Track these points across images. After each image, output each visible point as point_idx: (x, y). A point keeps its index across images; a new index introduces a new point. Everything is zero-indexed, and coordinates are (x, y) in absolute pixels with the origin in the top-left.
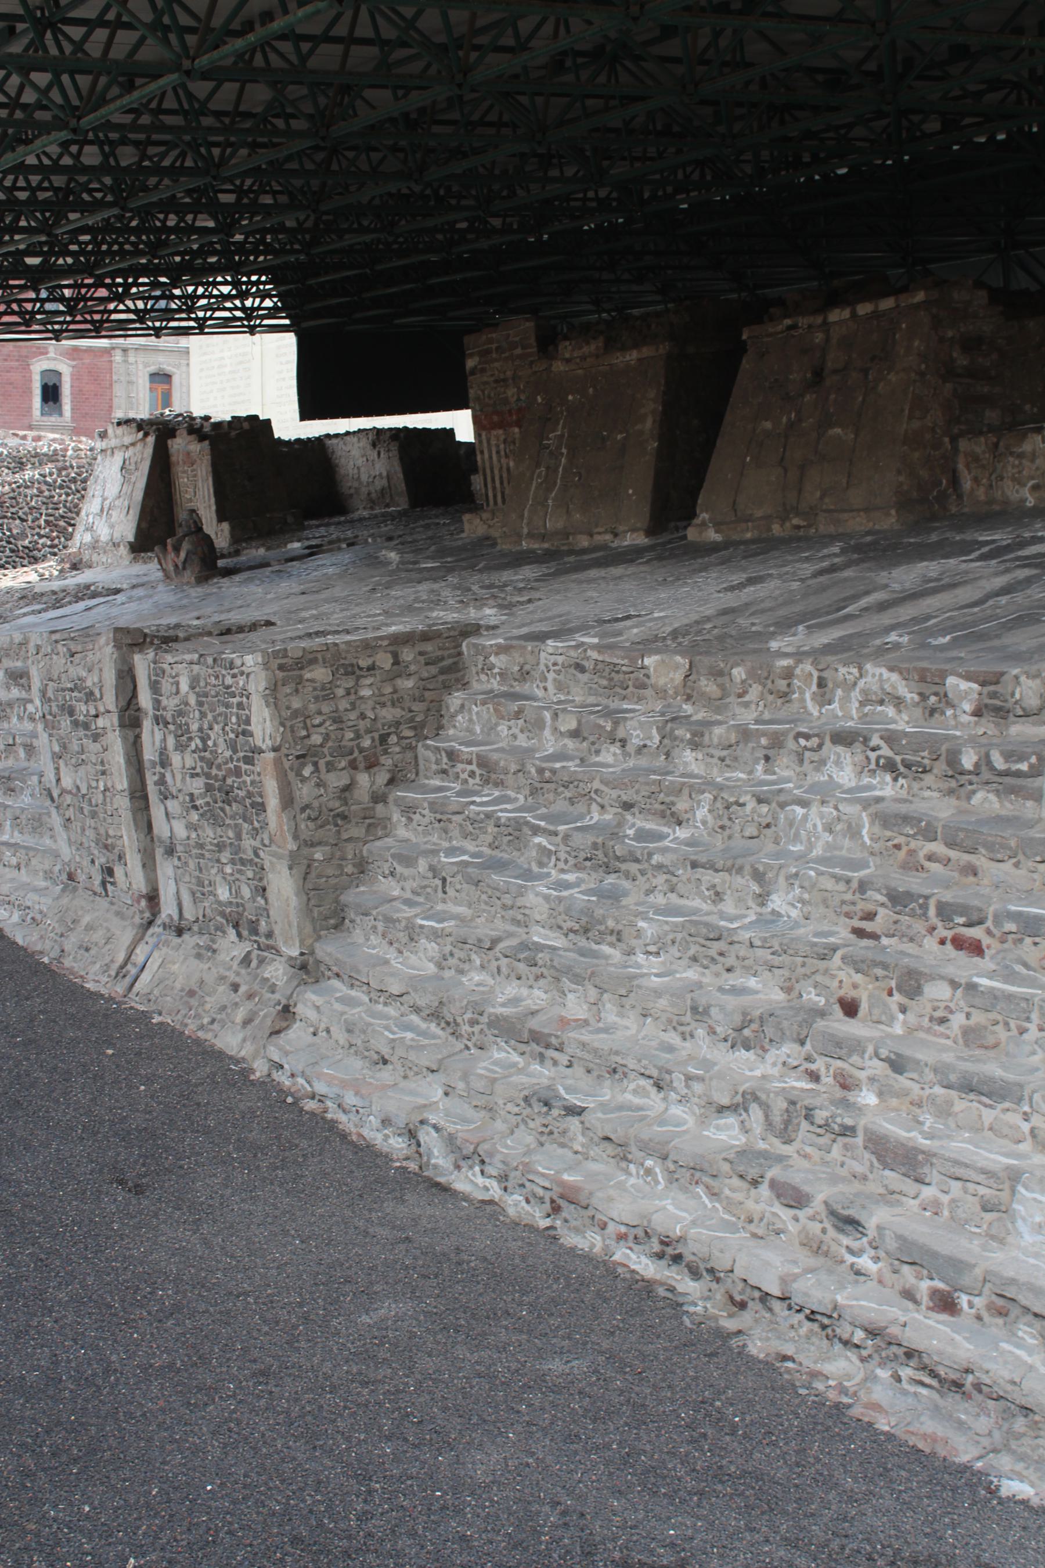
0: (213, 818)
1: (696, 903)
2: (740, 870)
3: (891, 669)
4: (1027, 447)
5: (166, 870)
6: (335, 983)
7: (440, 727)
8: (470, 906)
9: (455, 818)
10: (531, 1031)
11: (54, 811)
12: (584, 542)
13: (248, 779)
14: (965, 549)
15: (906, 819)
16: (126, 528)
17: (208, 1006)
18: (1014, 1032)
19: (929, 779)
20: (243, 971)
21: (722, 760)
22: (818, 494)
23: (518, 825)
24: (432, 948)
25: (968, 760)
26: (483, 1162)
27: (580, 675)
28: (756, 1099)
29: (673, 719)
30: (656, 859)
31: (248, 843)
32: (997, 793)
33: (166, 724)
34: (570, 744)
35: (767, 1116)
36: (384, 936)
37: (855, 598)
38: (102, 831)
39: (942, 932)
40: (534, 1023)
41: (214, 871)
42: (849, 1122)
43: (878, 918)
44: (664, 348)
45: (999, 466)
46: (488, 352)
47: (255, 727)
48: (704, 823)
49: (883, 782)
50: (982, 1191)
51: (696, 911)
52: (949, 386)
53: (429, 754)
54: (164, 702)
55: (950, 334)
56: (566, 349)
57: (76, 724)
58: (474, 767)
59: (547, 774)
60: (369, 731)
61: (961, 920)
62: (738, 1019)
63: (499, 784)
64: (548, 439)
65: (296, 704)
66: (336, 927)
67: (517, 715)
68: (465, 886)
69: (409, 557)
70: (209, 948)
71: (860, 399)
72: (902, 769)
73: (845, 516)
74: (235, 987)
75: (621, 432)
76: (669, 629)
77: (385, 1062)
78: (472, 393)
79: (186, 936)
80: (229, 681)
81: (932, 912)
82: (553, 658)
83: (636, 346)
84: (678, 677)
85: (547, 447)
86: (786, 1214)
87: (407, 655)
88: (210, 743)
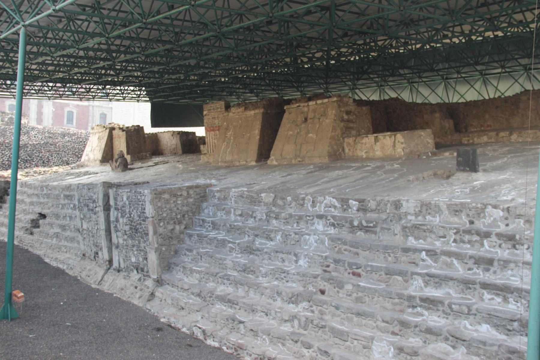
0: (132, 237)
1: (277, 263)
2: (290, 253)
3: (333, 198)
5: (115, 253)
6: (167, 286)
7: (200, 213)
8: (209, 264)
10: (228, 299)
11: (80, 236)
12: (237, 164)
13: (143, 226)
14: (350, 167)
15: (339, 239)
16: (99, 155)
17: (127, 293)
18: (371, 298)
19: (344, 228)
20: (139, 283)
21: (284, 223)
22: (305, 152)
23: (224, 241)
24: (198, 276)
25: (356, 223)
26: (214, 337)
27: (242, 199)
28: (296, 317)
29: (270, 212)
30: (265, 250)
31: (142, 245)
32: (364, 232)
33: (118, 210)
34: (239, 218)
35: (299, 323)
36: (183, 272)
37: (320, 180)
38: (95, 241)
39: (349, 271)
40: (229, 297)
41: (131, 253)
42: (324, 324)
43: (330, 267)
46: (210, 110)
47: (147, 211)
48: (279, 240)
49: (331, 229)
50: (363, 343)
51: (277, 265)
52: (342, 124)
53: (196, 220)
54: (118, 203)
55: (343, 109)
56: (233, 110)
57: (89, 210)
58: (210, 224)
60: (180, 213)
61: (354, 267)
62: (290, 295)
63: (218, 229)
65: (159, 204)
66: (168, 270)
67: (223, 210)
69: (186, 166)
70: (128, 276)
72: (336, 225)
74: (136, 287)
76: (267, 187)
77: (183, 309)
78: (205, 121)
79: (121, 272)
80: (139, 197)
81: (346, 265)
82: (234, 194)
83: (254, 109)
84: (271, 200)
86: (305, 351)
87: (191, 192)
88: (132, 215)
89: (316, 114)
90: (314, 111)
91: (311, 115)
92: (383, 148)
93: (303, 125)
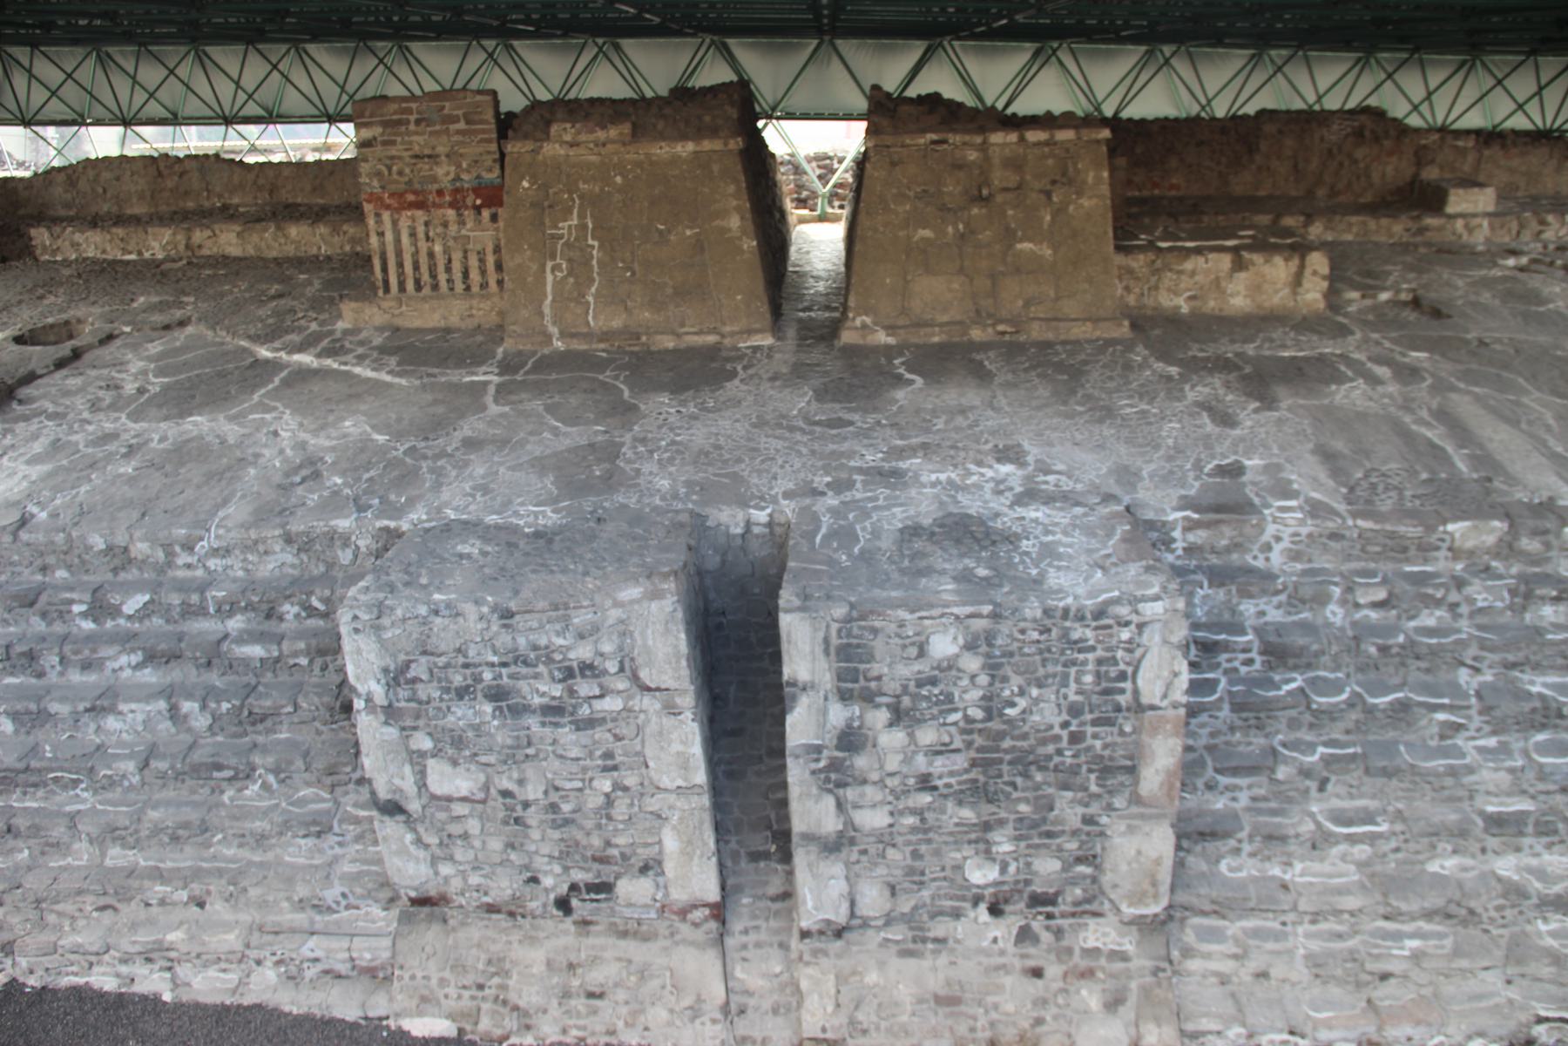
4: (1188, 265)
20: (1032, 950)
22: (1020, 303)
24: (1362, 851)
27: (1332, 544)
45: (1154, 279)
59: (1395, 650)
64: (556, 227)
67: (1277, 592)
68: (1366, 779)
70: (924, 940)
71: (1048, 218)
74: (1037, 973)
75: (691, 228)
83: (684, 137)
84: (1490, 540)
85: (561, 237)
89: (1028, 177)
90: (1015, 164)
91: (1000, 177)
92: (1255, 289)
93: (975, 211)
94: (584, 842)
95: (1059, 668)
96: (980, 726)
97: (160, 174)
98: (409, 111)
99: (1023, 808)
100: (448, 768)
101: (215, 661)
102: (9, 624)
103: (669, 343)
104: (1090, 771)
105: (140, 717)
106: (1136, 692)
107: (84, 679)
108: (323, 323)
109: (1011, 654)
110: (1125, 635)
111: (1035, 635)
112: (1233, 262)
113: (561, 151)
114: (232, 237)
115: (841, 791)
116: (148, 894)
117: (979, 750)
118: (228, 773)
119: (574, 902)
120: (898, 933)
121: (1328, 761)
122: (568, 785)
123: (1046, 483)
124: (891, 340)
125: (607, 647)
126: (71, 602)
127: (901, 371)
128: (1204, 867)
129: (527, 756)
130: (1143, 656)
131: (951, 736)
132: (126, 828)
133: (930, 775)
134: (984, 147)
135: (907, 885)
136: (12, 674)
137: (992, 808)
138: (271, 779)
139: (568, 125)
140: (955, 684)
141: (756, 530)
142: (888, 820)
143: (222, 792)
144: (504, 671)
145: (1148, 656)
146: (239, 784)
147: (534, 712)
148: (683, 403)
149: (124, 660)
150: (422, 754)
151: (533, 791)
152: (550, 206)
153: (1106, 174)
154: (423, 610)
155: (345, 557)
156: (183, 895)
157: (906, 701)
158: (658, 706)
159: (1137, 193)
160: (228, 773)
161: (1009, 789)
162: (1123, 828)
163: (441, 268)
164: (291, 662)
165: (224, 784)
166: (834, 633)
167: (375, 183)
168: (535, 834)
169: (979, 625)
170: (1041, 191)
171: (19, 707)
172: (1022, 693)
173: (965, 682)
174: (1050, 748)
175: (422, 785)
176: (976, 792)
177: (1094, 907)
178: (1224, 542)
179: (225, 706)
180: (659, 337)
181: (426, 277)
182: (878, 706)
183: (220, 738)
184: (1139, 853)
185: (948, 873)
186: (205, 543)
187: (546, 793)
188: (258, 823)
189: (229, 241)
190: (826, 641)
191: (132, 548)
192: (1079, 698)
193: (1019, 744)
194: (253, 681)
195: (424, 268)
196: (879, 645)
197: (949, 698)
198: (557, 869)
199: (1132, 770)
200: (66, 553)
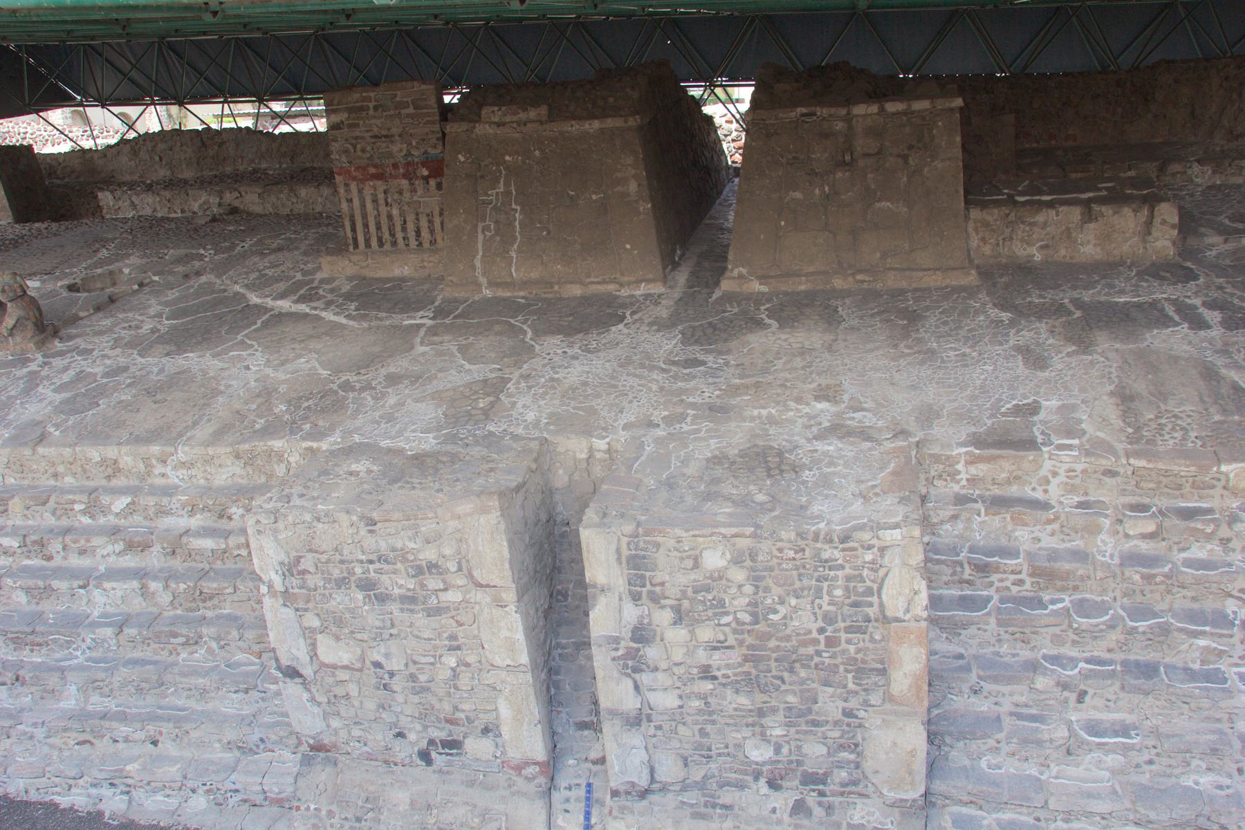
4: (1040, 218)
9: (1042, 630)
20: (805, 822)
22: (878, 255)
24: (1114, 760)
27: (1107, 480)
44: (633, 122)
67: (1049, 522)
68: (1122, 695)
70: (714, 806)
71: (905, 179)
73: (920, 274)
83: (592, 117)
89: (887, 144)
91: (862, 144)
93: (839, 175)
94: (437, 706)
95: (814, 582)
96: (749, 628)
97: (204, 145)
98: (369, 99)
99: (791, 699)
100: (332, 643)
101: (178, 551)
102: (29, 519)
103: (576, 291)
104: (847, 671)
105: (119, 593)
106: (881, 605)
107: (81, 562)
108: (305, 273)
109: (771, 569)
110: (869, 557)
111: (791, 554)
112: (1082, 214)
113: (490, 130)
114: (255, 197)
115: (637, 676)
116: (116, 733)
117: (748, 648)
118: (181, 640)
119: (434, 754)
120: (692, 797)
121: (1086, 676)
122: (424, 660)
123: (853, 418)
124: (764, 289)
125: (447, 551)
126: (74, 502)
127: (763, 316)
128: (967, 762)
129: (391, 635)
130: (887, 575)
131: (725, 635)
132: (103, 681)
133: (709, 666)
134: (848, 119)
135: (696, 758)
136: (28, 557)
137: (765, 698)
138: (214, 645)
139: (496, 108)
140: (725, 592)
141: (598, 455)
142: (678, 702)
143: (178, 654)
144: (371, 567)
145: (890, 575)
146: (190, 649)
147: (395, 600)
148: (571, 345)
149: (110, 548)
150: (313, 630)
151: (395, 664)
152: (482, 177)
153: (958, 139)
154: (308, 517)
155: (280, 470)
156: (141, 735)
157: (686, 604)
158: (488, 599)
159: (1035, 145)
160: (181, 640)
161: (778, 682)
162: (879, 722)
163: (398, 228)
164: (236, 554)
165: (179, 648)
166: (624, 546)
167: (344, 159)
168: (400, 698)
169: (743, 543)
170: (898, 156)
171: (31, 583)
172: (782, 602)
173: (734, 590)
174: (810, 650)
175: (314, 655)
176: (749, 683)
177: (860, 788)
178: (1004, 475)
179: (182, 586)
180: (569, 286)
181: (386, 236)
182: (663, 607)
183: (179, 612)
184: (895, 744)
185: (731, 750)
186: (174, 458)
187: (406, 665)
188: (201, 680)
189: (251, 200)
190: (618, 551)
191: (121, 461)
192: (832, 608)
193: (783, 644)
194: (207, 567)
195: (385, 229)
196: (661, 558)
197: (721, 603)
198: (418, 727)
199: (883, 672)
200: (71, 464)
